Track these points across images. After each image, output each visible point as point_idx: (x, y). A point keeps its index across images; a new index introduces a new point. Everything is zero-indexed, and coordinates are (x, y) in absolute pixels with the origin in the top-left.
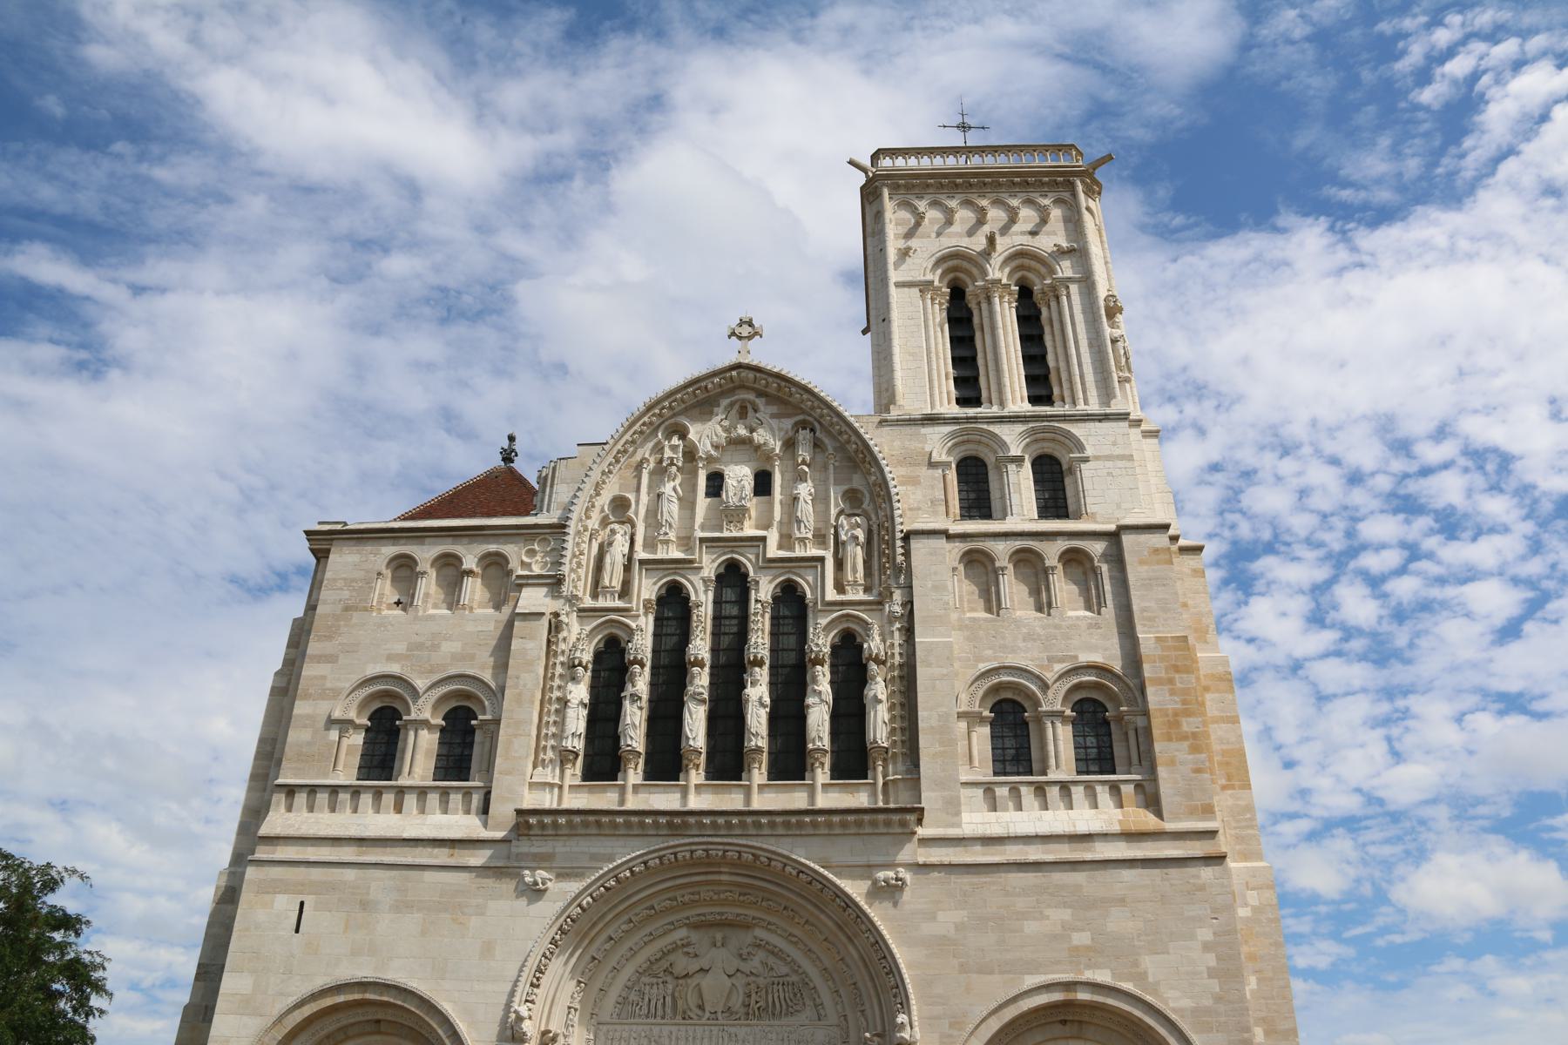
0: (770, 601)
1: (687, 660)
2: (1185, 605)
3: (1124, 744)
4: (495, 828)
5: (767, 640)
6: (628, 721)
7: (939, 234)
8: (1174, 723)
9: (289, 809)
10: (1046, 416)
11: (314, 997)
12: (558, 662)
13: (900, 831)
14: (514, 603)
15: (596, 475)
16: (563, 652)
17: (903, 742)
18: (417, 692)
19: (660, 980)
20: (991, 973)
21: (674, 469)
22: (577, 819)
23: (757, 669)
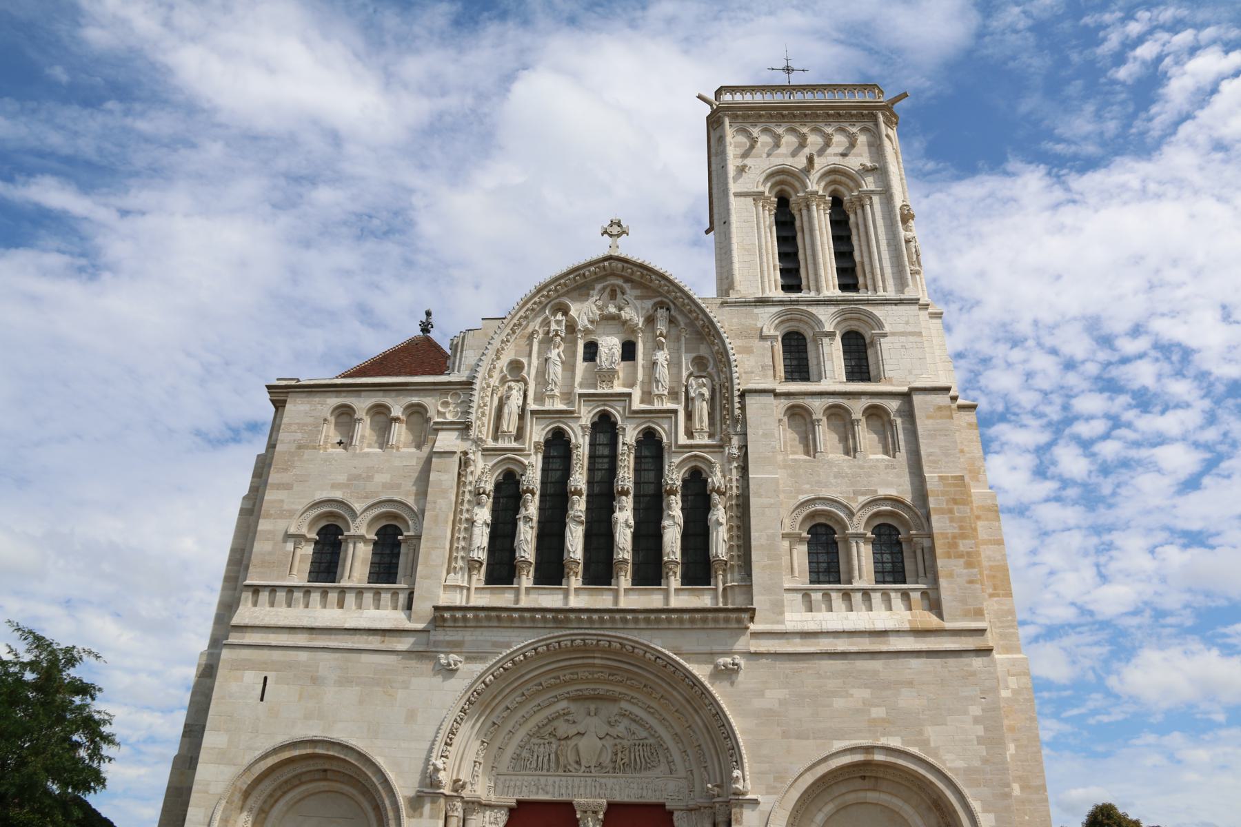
0: (634, 444)
1: (568, 490)
2: (962, 451)
3: (913, 560)
4: (417, 621)
5: (632, 475)
6: (522, 538)
7: (769, 155)
8: (953, 545)
9: (255, 604)
10: (854, 300)
11: (276, 751)
12: (466, 490)
13: (736, 626)
14: (431, 444)
15: (497, 343)
16: (471, 483)
17: (739, 556)
18: (356, 514)
19: (546, 741)
20: (808, 738)
21: (558, 339)
22: (482, 614)
23: (624, 498)
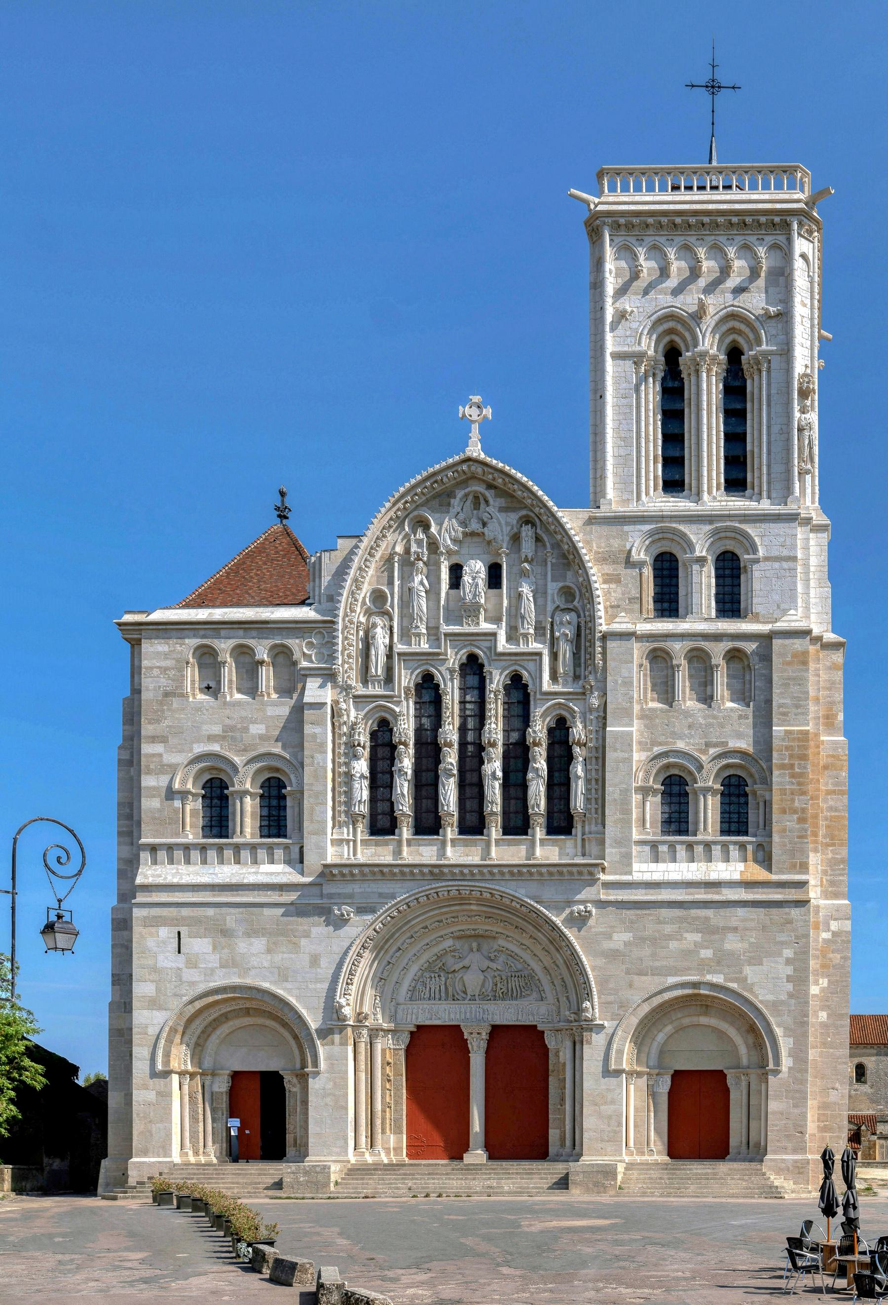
20: (646, 975)
21: (421, 564)
